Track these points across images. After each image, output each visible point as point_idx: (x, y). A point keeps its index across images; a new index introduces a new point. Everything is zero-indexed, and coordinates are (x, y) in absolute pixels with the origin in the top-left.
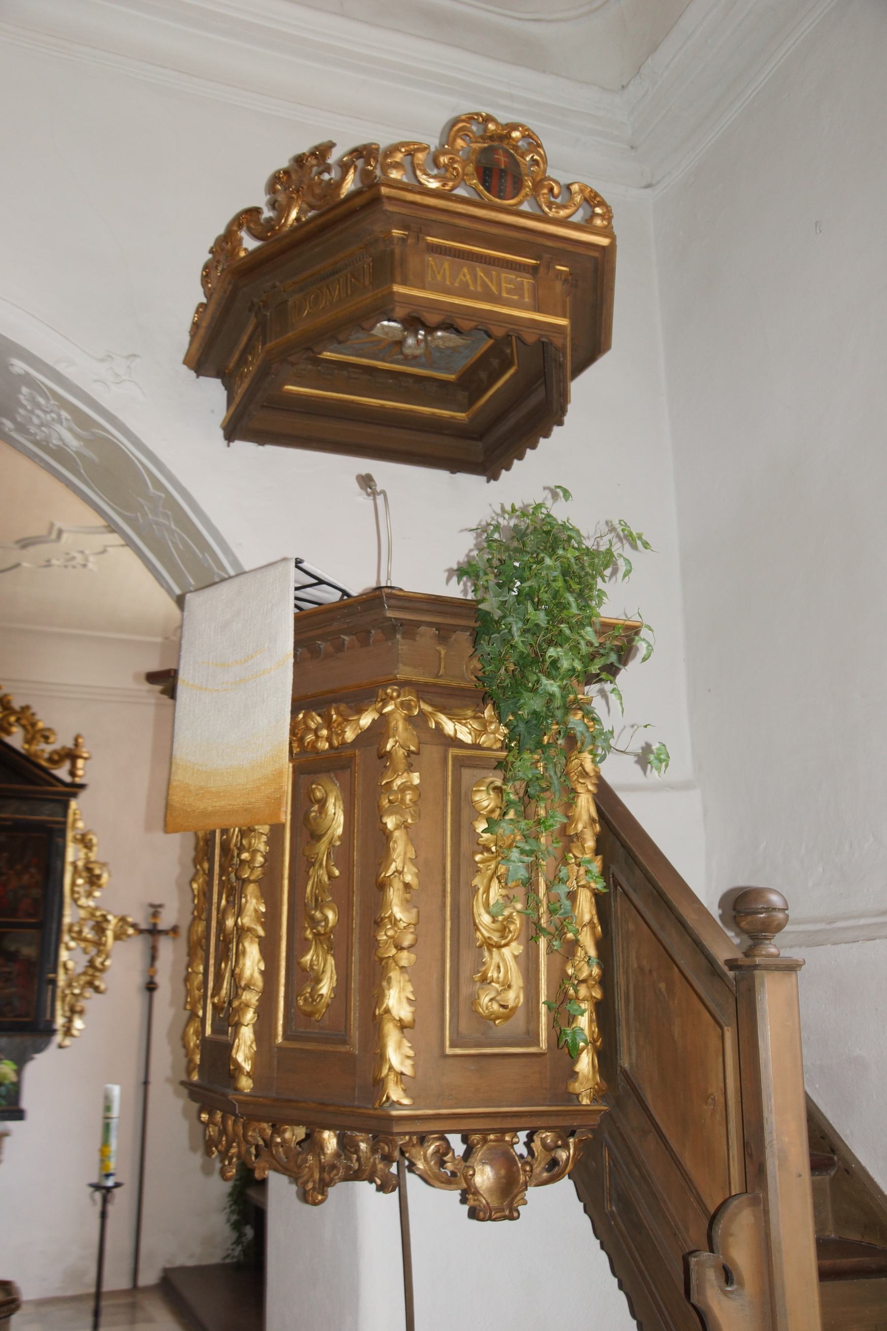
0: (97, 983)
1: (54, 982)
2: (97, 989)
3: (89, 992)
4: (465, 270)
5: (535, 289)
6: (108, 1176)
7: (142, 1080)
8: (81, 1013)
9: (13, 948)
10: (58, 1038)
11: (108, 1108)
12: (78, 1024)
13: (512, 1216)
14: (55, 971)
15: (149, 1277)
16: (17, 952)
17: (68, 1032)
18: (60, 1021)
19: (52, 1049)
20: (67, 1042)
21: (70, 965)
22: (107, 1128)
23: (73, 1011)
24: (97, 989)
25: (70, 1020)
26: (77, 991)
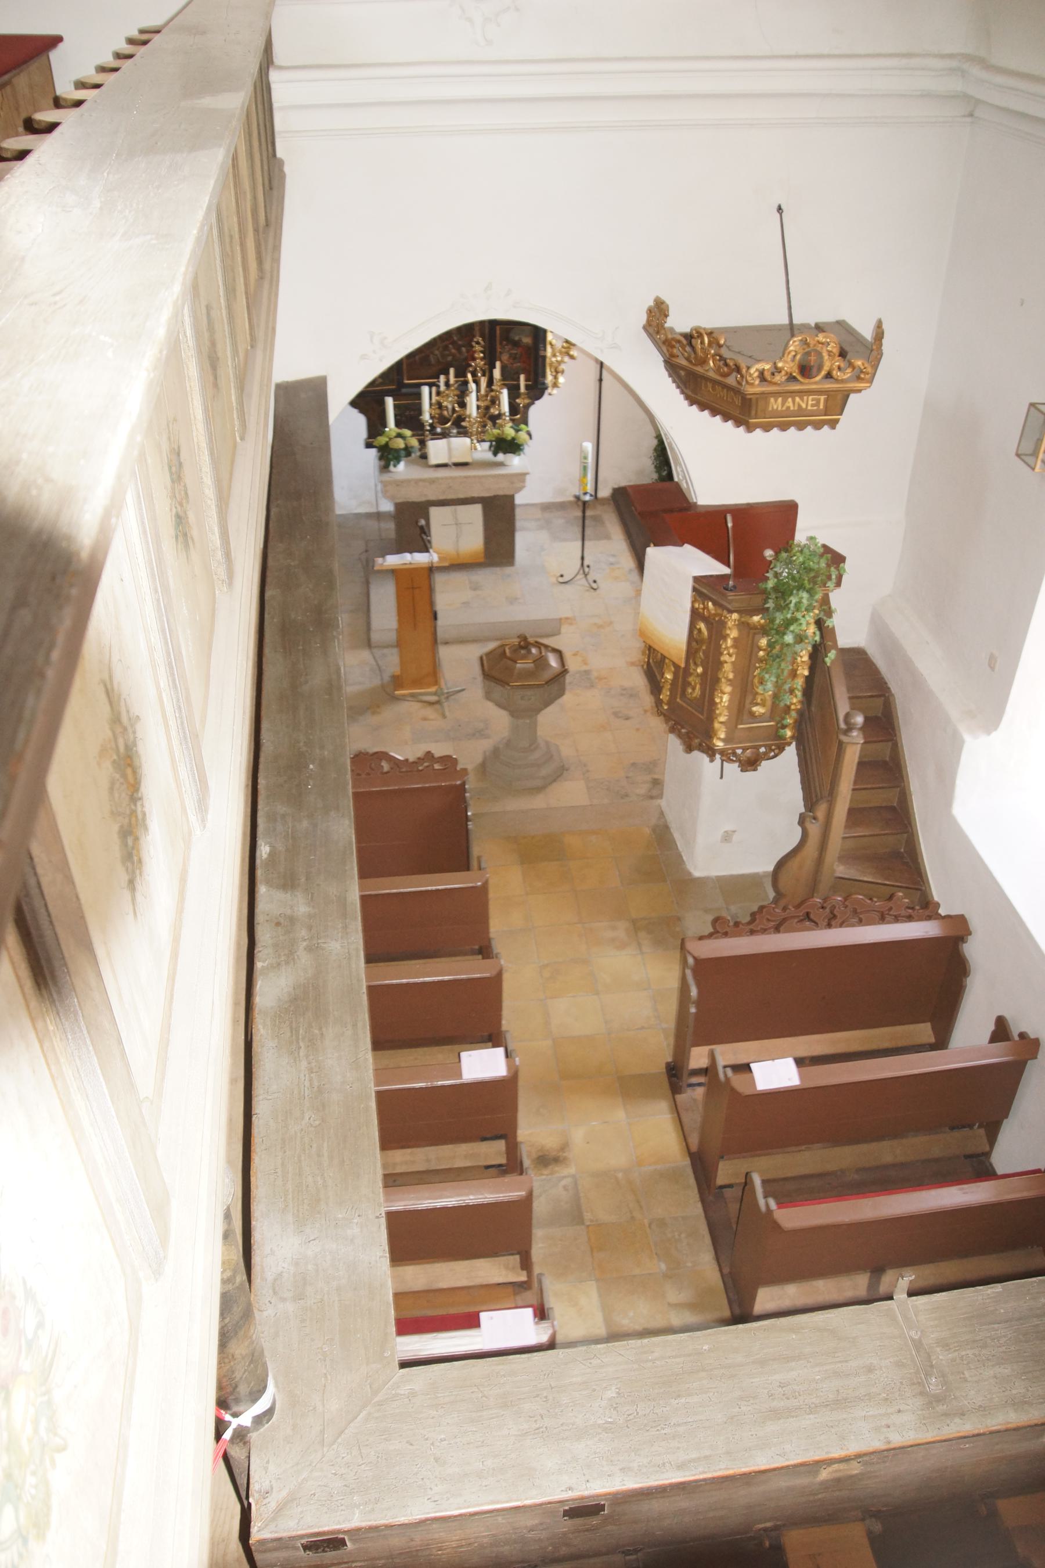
0: (571, 353)
1: (544, 358)
2: (572, 357)
3: (566, 359)
4: (790, 400)
5: (826, 401)
6: (585, 494)
7: (598, 377)
8: (563, 372)
9: (517, 338)
10: (549, 390)
11: (586, 458)
12: (561, 379)
13: (755, 770)
14: (545, 350)
15: (605, 492)
16: (520, 340)
17: (555, 385)
18: (549, 378)
19: (546, 396)
20: (555, 391)
21: (554, 342)
22: (585, 468)
23: (557, 372)
24: (572, 357)
25: (556, 378)
26: (559, 359)
